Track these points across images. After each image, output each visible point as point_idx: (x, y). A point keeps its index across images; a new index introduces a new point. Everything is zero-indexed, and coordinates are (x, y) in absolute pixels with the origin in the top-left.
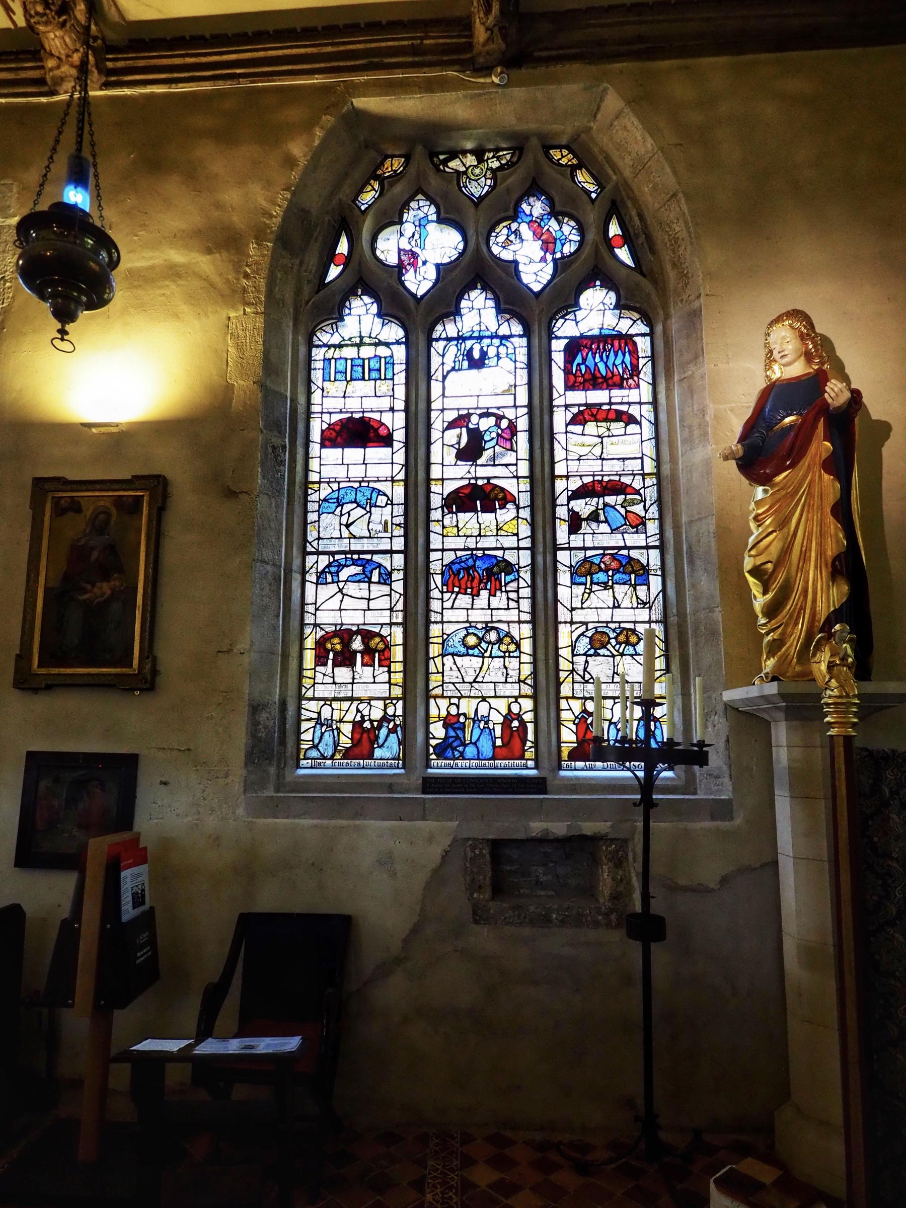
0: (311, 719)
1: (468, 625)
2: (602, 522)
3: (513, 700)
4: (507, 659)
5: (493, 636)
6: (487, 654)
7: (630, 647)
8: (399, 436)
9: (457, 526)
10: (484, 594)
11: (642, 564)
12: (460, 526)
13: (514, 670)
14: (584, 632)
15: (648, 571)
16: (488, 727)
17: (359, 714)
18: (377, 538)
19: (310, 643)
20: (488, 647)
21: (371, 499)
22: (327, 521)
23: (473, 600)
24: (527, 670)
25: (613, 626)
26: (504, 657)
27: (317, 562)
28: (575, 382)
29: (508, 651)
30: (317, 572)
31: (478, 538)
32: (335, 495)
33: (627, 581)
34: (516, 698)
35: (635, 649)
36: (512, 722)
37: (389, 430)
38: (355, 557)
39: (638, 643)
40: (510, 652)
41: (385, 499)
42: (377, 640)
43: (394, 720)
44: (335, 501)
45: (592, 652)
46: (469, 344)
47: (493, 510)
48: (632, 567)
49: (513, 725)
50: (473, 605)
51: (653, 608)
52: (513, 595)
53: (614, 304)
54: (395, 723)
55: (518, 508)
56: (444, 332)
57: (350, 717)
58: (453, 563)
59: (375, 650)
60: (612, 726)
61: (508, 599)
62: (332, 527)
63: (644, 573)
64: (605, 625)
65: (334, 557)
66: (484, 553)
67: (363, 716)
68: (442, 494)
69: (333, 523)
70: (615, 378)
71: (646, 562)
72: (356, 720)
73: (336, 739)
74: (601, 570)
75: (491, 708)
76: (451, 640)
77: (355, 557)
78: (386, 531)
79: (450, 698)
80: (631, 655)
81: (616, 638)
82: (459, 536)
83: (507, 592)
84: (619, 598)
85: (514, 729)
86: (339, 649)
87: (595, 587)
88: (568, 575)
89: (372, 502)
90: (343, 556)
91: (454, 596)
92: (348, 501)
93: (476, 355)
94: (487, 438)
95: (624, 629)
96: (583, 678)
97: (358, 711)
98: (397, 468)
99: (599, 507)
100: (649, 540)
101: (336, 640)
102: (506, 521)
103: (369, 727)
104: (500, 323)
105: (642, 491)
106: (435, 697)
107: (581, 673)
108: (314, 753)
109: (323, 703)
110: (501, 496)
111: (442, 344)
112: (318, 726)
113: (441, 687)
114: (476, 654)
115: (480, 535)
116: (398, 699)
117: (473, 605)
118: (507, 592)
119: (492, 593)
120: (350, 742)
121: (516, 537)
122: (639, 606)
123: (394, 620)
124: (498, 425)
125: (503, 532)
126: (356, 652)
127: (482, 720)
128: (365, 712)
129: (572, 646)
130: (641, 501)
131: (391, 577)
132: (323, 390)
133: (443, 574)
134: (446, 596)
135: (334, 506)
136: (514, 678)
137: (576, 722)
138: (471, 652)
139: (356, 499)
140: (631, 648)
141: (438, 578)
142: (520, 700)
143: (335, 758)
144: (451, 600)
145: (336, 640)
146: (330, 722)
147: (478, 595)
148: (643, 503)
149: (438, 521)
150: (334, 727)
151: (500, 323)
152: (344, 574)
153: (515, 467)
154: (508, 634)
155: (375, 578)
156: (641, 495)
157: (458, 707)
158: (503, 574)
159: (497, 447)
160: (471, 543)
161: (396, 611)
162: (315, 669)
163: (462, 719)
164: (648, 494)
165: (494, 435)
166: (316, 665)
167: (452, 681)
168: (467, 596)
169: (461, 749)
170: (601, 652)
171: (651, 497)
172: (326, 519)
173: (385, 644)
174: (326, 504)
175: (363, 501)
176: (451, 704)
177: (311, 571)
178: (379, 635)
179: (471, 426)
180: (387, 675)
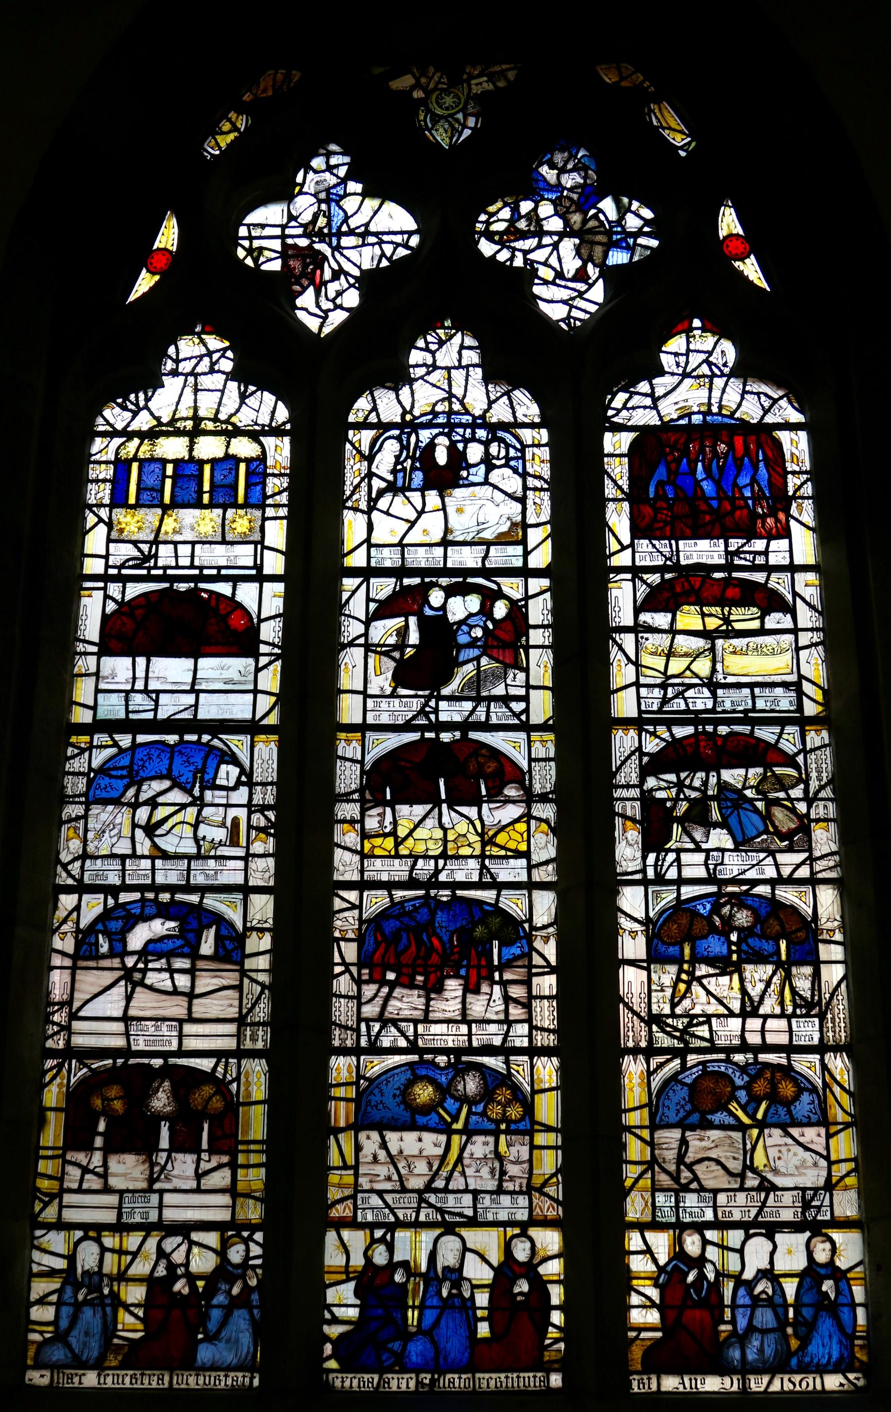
0: (52, 1273)
1: (415, 1058)
2: (716, 825)
3: (517, 1231)
4: (502, 1138)
5: (471, 1085)
6: (459, 1126)
7: (780, 1109)
8: (270, 632)
9: (394, 833)
10: (453, 986)
11: (803, 918)
12: (402, 832)
13: (517, 1162)
14: (677, 1074)
15: (817, 931)
16: (460, 1295)
17: (163, 1264)
18: (216, 857)
19: (52, 1096)
20: (459, 1110)
21: (203, 771)
22: (104, 817)
23: (428, 1000)
24: (548, 1162)
25: (739, 1058)
26: (496, 1134)
27: (77, 908)
28: (654, 520)
29: (505, 1119)
30: (78, 930)
31: (441, 862)
32: (125, 761)
33: (771, 955)
34: (524, 1227)
35: (789, 1112)
36: (513, 1283)
37: (252, 618)
38: (165, 897)
39: (797, 1097)
40: (509, 1122)
41: (234, 771)
42: (207, 1090)
43: (243, 1277)
44: (124, 772)
45: (695, 1118)
46: (425, 435)
47: (477, 802)
48: (782, 924)
49: (516, 1290)
50: (427, 1011)
51: (829, 1016)
52: (517, 992)
53: (730, 364)
54: (245, 1284)
55: (530, 798)
56: (374, 413)
57: (141, 1268)
58: (383, 915)
59: (203, 1114)
60: (742, 1291)
61: (507, 999)
62: (116, 831)
63: (807, 937)
64: (722, 1056)
65: (116, 898)
66: (454, 895)
67: (171, 1267)
68: (362, 762)
69: (118, 821)
70: (738, 513)
71: (810, 911)
72: (156, 1275)
73: (109, 1319)
74: (713, 930)
75: (465, 1249)
76: (376, 1091)
77: (165, 897)
78: (234, 841)
79: (371, 1226)
80: (784, 1127)
81: (748, 1087)
82: (398, 856)
83: (504, 984)
84: (755, 991)
85: (519, 1298)
86: (121, 1112)
87: (702, 970)
88: (641, 940)
89: (207, 777)
90: (137, 896)
91: (385, 990)
92: (153, 773)
93: (441, 457)
94: (463, 639)
95: (767, 1065)
96: (676, 1178)
97: (161, 1253)
98: (265, 703)
99: (710, 793)
100: (819, 866)
101: (114, 1091)
102: (504, 823)
103: (186, 1291)
104: (493, 397)
105: (800, 759)
106: (340, 1224)
107: (672, 1168)
108: (58, 1354)
109: (79, 1234)
110: (491, 767)
111: (367, 436)
112: (69, 1291)
113: (350, 1203)
114: (432, 1124)
115: (444, 855)
116: (253, 1228)
117: (427, 1011)
118: (504, 984)
119: (471, 987)
120: (141, 1327)
121: (523, 862)
122: (798, 1012)
123: (248, 1045)
124: (486, 611)
125: (495, 849)
126: (158, 1117)
127: (445, 1279)
128: (178, 1257)
129: (649, 1105)
130: (799, 780)
131: (243, 946)
132: (110, 525)
133: (360, 939)
134: (369, 990)
135: (120, 784)
136: (518, 1181)
137: (661, 1280)
138: (421, 1120)
139: (170, 770)
140: (782, 1111)
141: (350, 951)
142: (533, 1232)
143: (107, 1364)
144: (379, 1001)
145: (114, 1091)
146: (96, 1279)
147: (440, 989)
148: (802, 786)
149: (352, 822)
150: (106, 1291)
151: (493, 397)
152: (138, 938)
153: (522, 706)
154: (506, 1079)
155: (207, 947)
156: (797, 767)
157: (390, 1248)
158: (496, 943)
159: (484, 661)
160: (425, 868)
161: (252, 1024)
162: (63, 1156)
163: (398, 1277)
164: (814, 766)
165: (478, 633)
166: (66, 1148)
167: (378, 1186)
168: (416, 992)
169: (396, 1346)
170: (719, 1117)
171: (819, 772)
172: (101, 815)
173: (224, 1098)
174: (104, 781)
175: (187, 776)
176: (373, 1241)
177: (65, 928)
178: (209, 1077)
179: (428, 612)
180: (227, 1173)
